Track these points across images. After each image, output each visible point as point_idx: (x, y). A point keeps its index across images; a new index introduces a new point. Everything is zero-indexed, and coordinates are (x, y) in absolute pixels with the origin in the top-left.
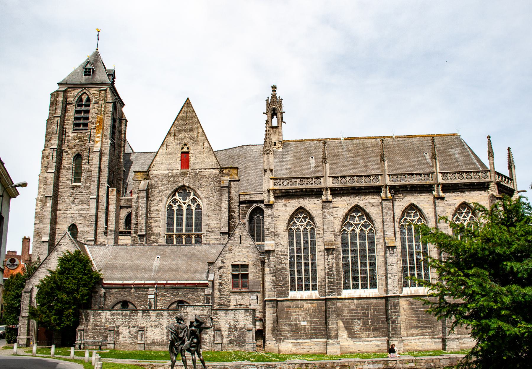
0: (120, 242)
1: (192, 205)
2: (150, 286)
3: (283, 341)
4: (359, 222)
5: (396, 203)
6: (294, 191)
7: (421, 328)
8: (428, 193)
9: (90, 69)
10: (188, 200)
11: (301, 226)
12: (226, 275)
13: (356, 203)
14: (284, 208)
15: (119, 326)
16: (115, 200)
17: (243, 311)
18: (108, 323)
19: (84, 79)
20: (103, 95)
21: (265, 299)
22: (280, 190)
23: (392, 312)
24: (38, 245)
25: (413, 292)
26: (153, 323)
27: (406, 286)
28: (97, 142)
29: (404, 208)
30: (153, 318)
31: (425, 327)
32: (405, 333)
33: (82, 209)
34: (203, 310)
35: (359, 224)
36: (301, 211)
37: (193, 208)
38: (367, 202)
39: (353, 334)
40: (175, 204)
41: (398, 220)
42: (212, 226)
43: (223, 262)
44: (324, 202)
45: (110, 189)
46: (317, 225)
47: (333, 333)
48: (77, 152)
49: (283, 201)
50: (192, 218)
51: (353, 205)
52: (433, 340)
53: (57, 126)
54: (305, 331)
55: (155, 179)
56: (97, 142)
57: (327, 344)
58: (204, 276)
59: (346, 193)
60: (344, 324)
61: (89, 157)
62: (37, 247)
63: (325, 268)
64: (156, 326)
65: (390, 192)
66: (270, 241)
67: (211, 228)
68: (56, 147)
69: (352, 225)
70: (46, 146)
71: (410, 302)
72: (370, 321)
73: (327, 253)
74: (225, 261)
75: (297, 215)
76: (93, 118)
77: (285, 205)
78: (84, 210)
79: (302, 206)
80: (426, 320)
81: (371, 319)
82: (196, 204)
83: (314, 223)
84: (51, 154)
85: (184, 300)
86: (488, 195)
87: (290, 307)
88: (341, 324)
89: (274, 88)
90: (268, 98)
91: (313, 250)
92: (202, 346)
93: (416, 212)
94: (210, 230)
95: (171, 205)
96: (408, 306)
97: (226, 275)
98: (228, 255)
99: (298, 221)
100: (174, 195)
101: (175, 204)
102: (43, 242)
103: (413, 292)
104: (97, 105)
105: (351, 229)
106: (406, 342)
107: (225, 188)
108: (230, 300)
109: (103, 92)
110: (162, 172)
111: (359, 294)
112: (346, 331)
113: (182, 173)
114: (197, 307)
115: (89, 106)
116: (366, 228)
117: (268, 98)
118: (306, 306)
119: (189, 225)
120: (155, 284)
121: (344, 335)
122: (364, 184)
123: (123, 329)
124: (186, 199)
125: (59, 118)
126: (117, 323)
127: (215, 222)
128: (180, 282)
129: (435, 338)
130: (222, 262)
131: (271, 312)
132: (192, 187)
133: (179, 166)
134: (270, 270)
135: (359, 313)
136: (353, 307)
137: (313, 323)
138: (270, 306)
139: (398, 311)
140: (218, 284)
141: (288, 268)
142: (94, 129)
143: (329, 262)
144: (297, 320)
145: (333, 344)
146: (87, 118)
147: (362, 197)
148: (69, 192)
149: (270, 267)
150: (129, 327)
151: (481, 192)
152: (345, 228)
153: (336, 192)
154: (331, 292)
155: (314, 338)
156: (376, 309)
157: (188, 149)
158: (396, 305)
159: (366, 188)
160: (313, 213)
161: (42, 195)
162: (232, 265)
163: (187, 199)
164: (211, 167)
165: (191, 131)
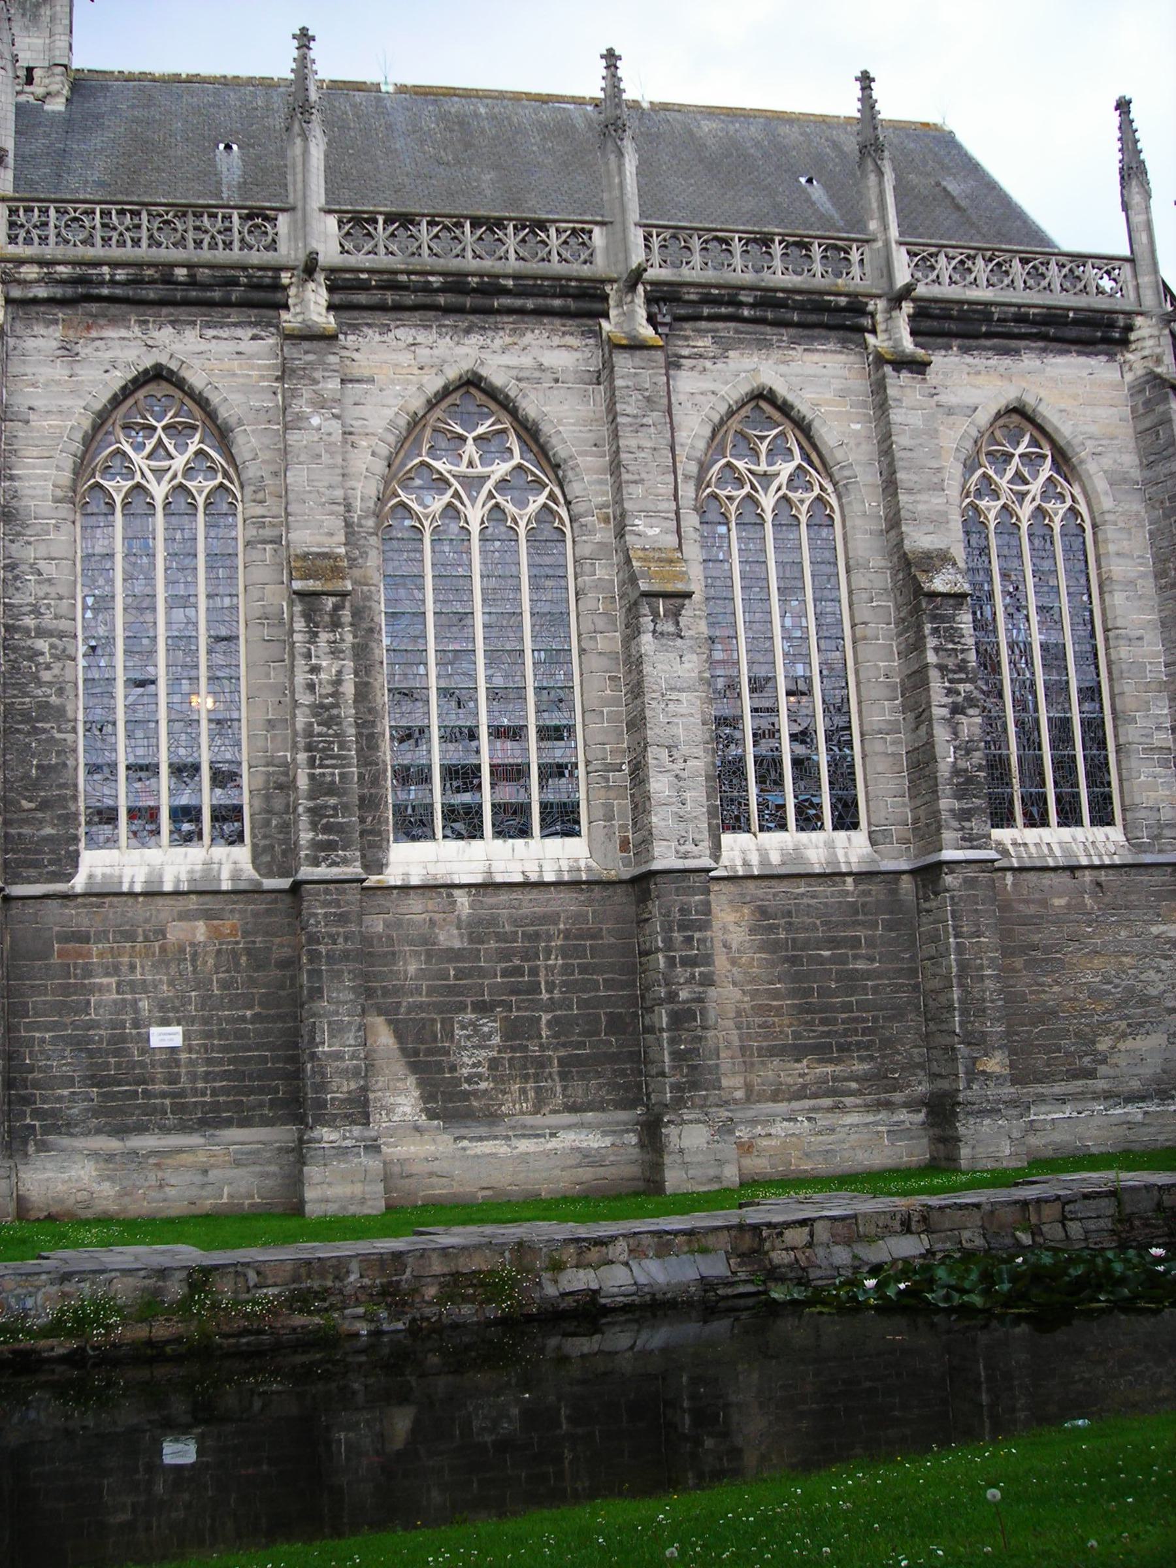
3: (43, 1147)
4: (480, 470)
5: (686, 382)
6: (121, 275)
7: (821, 1052)
8: (844, 342)
11: (159, 473)
14: (59, 371)
22: (41, 263)
23: (671, 962)
25: (775, 858)
27: (738, 824)
29: (723, 408)
31: (842, 1048)
32: (738, 1081)
35: (484, 478)
36: (160, 389)
39: (449, 1097)
41: (693, 468)
46: (252, 472)
47: (341, 1088)
49: (57, 332)
51: (452, 373)
52: (882, 1115)
54: (173, 1079)
57: (299, 1154)
60: (399, 1036)
63: (295, 704)
65: (651, 319)
71: (763, 912)
72: (545, 1017)
73: (308, 616)
77: (67, 350)
79: (164, 360)
80: (847, 1007)
81: (551, 1006)
83: (231, 458)
86: (1129, 377)
87: (84, 938)
88: (384, 1038)
93: (782, 434)
96: (752, 931)
99: (139, 447)
103: (775, 858)
106: (742, 1133)
111: (481, 867)
112: (411, 1080)
116: (522, 504)
118: (176, 932)
121: (403, 1102)
129: (889, 1105)
135: (482, 973)
136: (450, 938)
137: (222, 1034)
139: (707, 960)
143: (315, 670)
144: (128, 1018)
145: (343, 1152)
147: (501, 340)
151: (1092, 361)
152: (404, 497)
153: (362, 298)
154: (330, 846)
155: (228, 1123)
156: (578, 952)
158: (695, 923)
159: (527, 286)
160: (231, 403)
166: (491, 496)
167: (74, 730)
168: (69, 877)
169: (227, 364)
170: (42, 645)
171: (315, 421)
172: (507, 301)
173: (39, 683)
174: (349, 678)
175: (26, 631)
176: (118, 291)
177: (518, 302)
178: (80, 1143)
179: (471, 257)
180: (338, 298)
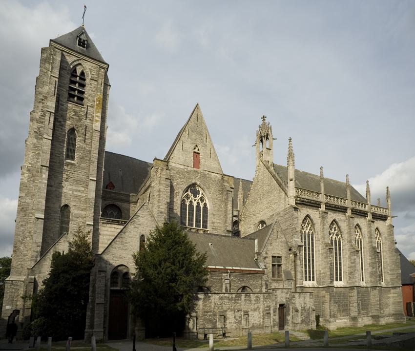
1: (200, 202)
10: (197, 198)
15: (226, 311)
18: (216, 308)
26: (252, 307)
30: (253, 302)
33: (76, 190)
37: (202, 206)
42: (216, 224)
43: (266, 253)
48: (72, 126)
50: (200, 214)
53: (55, 88)
55: (173, 172)
61: (85, 135)
62: (22, 225)
64: (255, 310)
74: (268, 252)
76: (90, 95)
78: (79, 191)
82: (203, 203)
98: (270, 247)
102: (38, 218)
113: (195, 171)
119: (198, 221)
123: (230, 315)
124: (196, 197)
126: (225, 308)
127: (218, 221)
132: (202, 186)
146: (83, 93)
150: (235, 312)
157: (198, 150)
161: (30, 164)
162: (273, 257)
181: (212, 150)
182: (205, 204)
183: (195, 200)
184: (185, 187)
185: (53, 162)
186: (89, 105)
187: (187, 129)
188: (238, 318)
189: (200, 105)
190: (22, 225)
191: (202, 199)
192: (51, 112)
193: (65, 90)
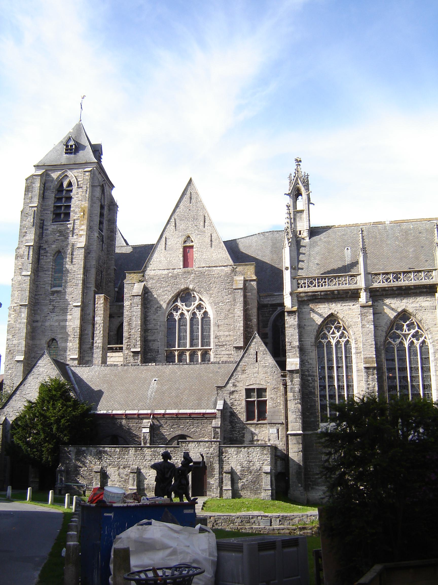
0: (110, 361)
2: (145, 416)
3: (313, 488)
4: (407, 332)
9: (71, 146)
11: (333, 338)
12: (239, 402)
13: (403, 308)
16: (102, 308)
17: (258, 449)
19: (64, 158)
20: (87, 177)
21: (288, 433)
22: (305, 293)
24: (11, 366)
28: (81, 235)
34: (209, 447)
37: (199, 316)
38: (418, 305)
40: (177, 312)
42: (222, 339)
43: (234, 385)
44: (363, 307)
45: (97, 296)
48: (57, 249)
50: (198, 328)
56: (81, 235)
58: (211, 404)
59: (390, 295)
66: (293, 358)
67: (222, 342)
68: (32, 244)
69: (399, 337)
70: (20, 242)
75: (327, 324)
76: (77, 206)
79: (333, 312)
84: (26, 253)
85: (186, 434)
89: (298, 161)
90: (291, 174)
91: (349, 368)
92: (208, 493)
94: (220, 344)
95: (172, 313)
97: (239, 402)
100: (176, 301)
101: (177, 312)
102: (18, 361)
104: (80, 190)
105: (398, 341)
107: (239, 291)
108: (244, 434)
109: (87, 174)
110: (161, 272)
113: (185, 272)
114: (201, 443)
115: (71, 191)
116: (418, 340)
117: (291, 174)
120: (151, 414)
122: (413, 282)
125: (36, 209)
127: (227, 333)
128: (181, 411)
130: (233, 385)
131: (296, 450)
132: (197, 289)
133: (182, 263)
134: (294, 396)
138: (295, 441)
140: (229, 414)
141: (318, 392)
142: (77, 219)
143: (369, 384)
148: (48, 298)
149: (294, 392)
152: (390, 340)
153: (378, 294)
161: (16, 303)
163: (191, 305)
164: (221, 265)
165: (195, 219)
166: (410, 339)
167: (318, 397)
168: (317, 430)
169: (347, 312)
170: (310, 378)
171: (368, 326)
172: (412, 291)
173: (310, 387)
174: (376, 386)
175: (306, 375)
176: (322, 297)
177: (415, 291)
178: (320, 488)
179: (403, 282)
180: (372, 294)
181: (214, 236)
182: (206, 313)
183: (188, 311)
184: (170, 297)
185: (38, 295)
186: (75, 218)
187: (173, 220)
188: (124, 476)
189: (193, 179)
190: (10, 369)
191: (199, 307)
192: (29, 246)
193: (50, 212)
